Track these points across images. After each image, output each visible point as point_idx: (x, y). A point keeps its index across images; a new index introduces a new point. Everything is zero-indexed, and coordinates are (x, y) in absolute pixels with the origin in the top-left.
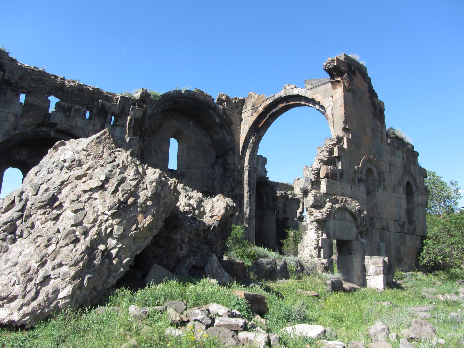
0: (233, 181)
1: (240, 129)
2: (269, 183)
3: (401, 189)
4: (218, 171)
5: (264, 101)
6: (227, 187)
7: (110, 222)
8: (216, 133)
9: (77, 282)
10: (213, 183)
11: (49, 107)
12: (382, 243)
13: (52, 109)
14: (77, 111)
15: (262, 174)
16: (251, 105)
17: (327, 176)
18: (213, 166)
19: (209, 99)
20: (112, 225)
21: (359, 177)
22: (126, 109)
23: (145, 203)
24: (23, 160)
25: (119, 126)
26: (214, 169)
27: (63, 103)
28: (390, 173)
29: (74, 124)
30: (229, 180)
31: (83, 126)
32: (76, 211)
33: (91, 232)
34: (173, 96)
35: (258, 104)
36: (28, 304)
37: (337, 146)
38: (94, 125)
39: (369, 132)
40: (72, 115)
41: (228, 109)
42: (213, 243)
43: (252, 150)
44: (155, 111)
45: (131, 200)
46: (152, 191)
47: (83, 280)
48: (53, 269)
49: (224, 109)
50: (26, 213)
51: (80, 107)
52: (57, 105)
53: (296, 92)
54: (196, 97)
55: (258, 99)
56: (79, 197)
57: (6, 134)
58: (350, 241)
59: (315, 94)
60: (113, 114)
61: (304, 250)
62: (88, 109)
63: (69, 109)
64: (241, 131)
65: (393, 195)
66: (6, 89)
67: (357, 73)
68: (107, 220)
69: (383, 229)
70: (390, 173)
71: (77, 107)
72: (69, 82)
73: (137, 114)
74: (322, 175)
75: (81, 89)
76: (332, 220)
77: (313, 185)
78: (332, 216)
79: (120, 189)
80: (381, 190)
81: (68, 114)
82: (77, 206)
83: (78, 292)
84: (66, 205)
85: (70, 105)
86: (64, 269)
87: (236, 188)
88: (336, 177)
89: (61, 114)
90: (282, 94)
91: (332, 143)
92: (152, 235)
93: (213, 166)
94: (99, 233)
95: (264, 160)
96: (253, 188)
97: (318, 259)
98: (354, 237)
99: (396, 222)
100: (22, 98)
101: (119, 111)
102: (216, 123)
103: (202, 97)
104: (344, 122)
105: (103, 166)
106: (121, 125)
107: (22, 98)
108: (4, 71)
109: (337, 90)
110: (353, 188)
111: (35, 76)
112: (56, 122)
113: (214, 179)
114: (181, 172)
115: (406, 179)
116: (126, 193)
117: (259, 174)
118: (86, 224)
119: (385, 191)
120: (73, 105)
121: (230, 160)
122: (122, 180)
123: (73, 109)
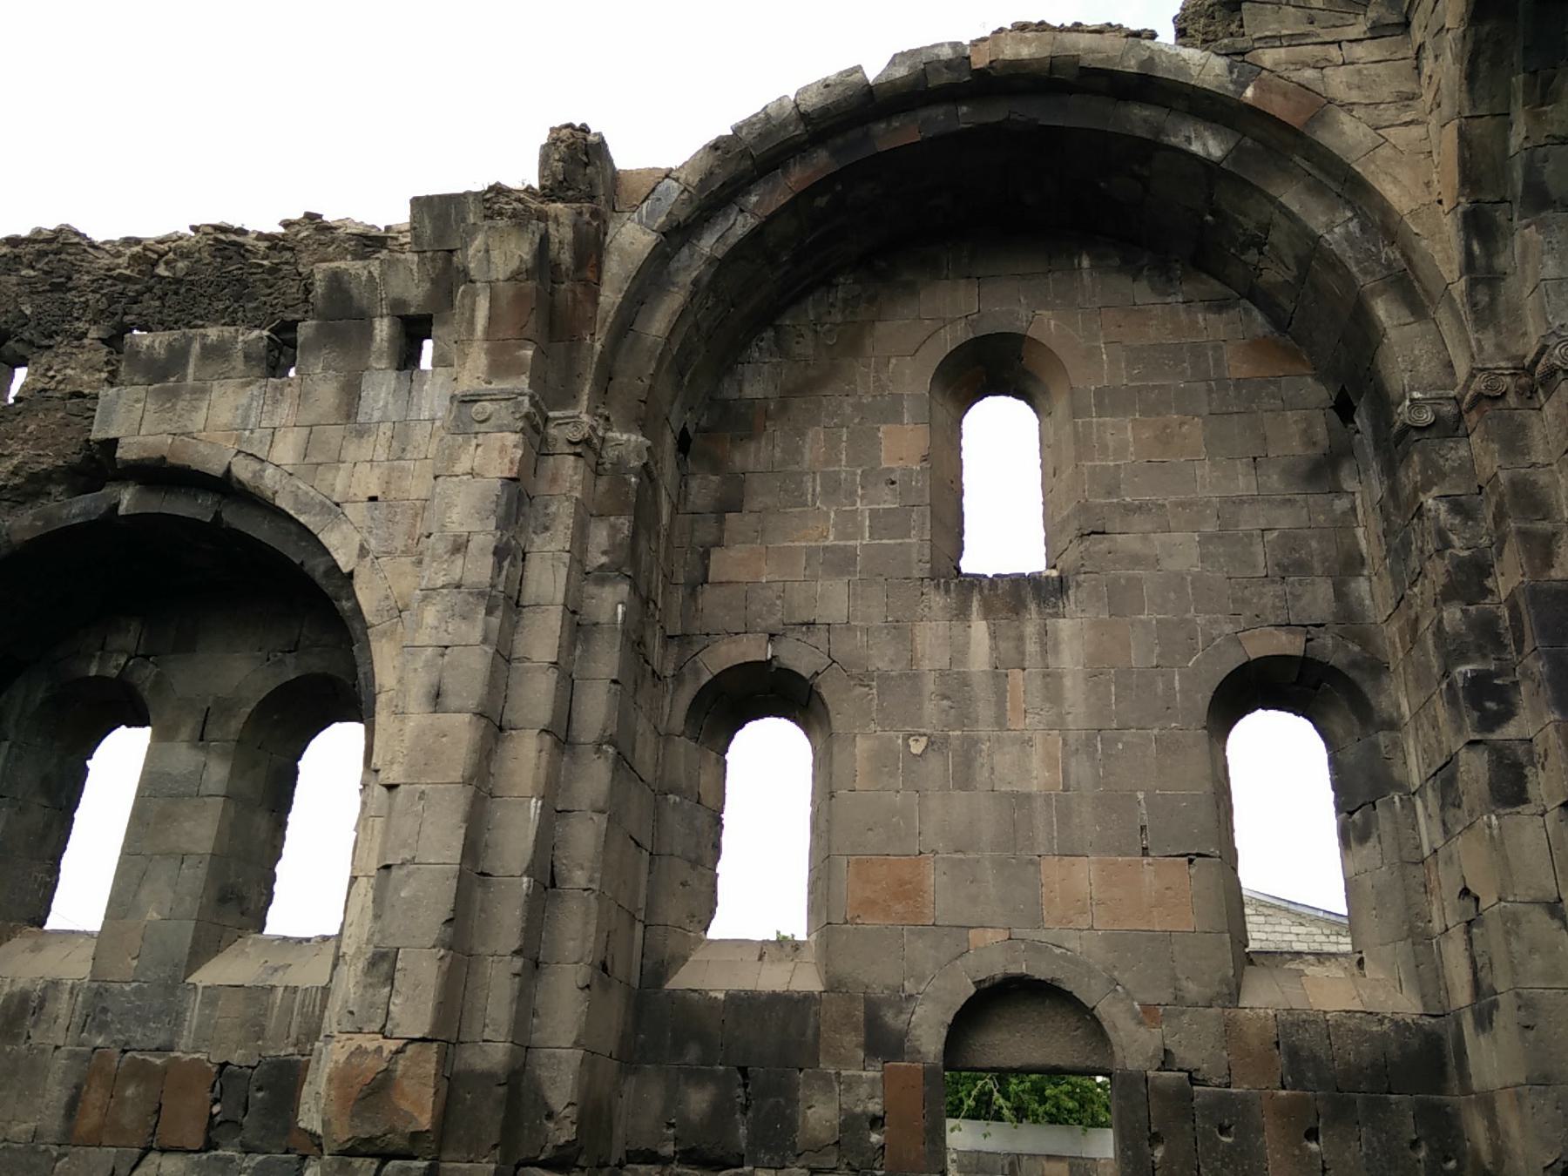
0: (1457, 506)
8: (1259, 244)
10: (1340, 594)
18: (1321, 472)
24: (114, 673)
26: (1338, 491)
30: (1420, 512)
38: (302, 397)
40: (190, 380)
54: (980, 61)
71: (213, 333)
73: (496, 255)
89: (140, 391)
102: (1205, 163)
103: (1025, 52)
111: (33, 268)
112: (112, 434)
113: (1352, 563)
123: (196, 347)
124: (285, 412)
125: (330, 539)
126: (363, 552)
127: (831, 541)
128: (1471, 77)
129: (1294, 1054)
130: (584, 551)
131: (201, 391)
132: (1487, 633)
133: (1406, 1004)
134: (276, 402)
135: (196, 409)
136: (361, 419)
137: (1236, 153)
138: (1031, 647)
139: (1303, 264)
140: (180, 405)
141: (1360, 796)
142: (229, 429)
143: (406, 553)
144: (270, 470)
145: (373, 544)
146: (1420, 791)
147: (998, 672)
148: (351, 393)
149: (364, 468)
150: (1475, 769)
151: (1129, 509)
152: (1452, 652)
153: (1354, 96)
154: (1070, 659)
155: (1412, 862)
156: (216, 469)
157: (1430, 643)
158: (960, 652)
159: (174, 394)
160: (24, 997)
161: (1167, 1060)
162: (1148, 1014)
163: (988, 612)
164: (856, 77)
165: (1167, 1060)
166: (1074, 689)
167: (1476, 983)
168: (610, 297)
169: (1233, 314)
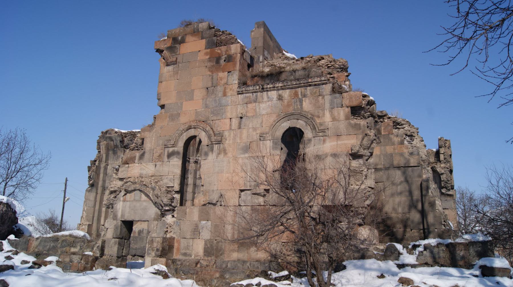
3: (269, 144)
12: (204, 222)
28: (240, 128)
39: (199, 94)
65: (242, 156)
67: (189, 38)
69: (214, 205)
70: (240, 128)
76: (121, 203)
80: (211, 157)
88: (135, 159)
98: (153, 216)
99: (249, 192)
108: (112, 140)
110: (157, 166)
115: (286, 125)
119: (222, 156)
130: (196, 175)
160: (140, 230)
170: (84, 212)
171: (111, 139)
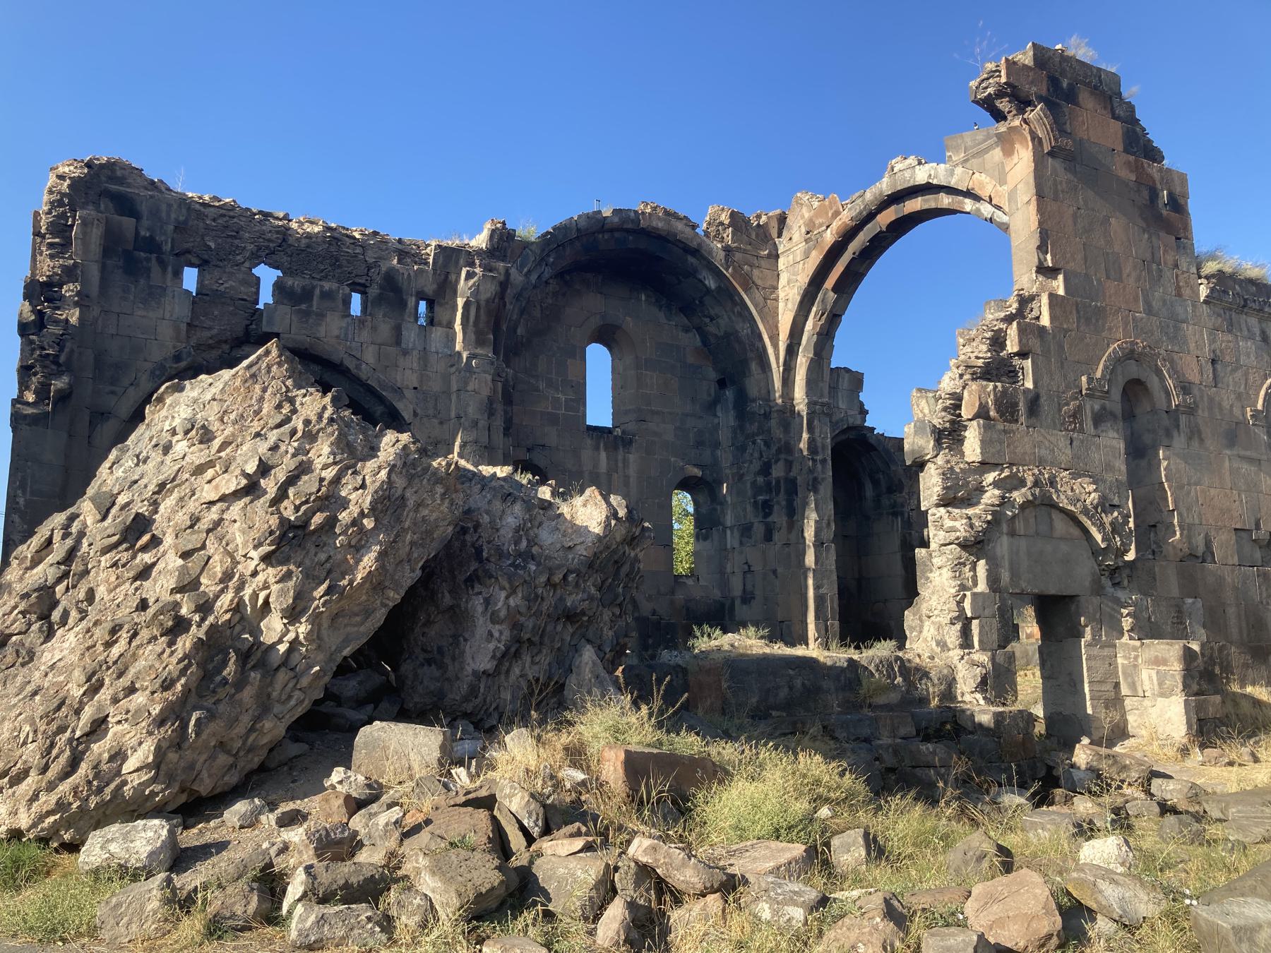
0: (767, 444)
1: (776, 300)
2: (872, 441)
4: (726, 419)
5: (837, 214)
6: (751, 462)
7: (261, 578)
9: (168, 730)
11: (257, 293)
13: (266, 297)
14: (327, 295)
15: (851, 420)
16: (803, 230)
17: (982, 413)
19: (680, 226)
20: (266, 586)
21: (1097, 407)
22: (453, 277)
23: (354, 522)
25: (440, 324)
26: (715, 415)
27: (290, 282)
29: (322, 332)
30: (754, 443)
31: (346, 334)
32: (185, 555)
33: (218, 604)
34: (578, 230)
35: (821, 225)
36: (51, 787)
37: (1015, 323)
41: (738, 249)
42: (585, 618)
43: (815, 354)
44: (534, 278)
45: (318, 519)
46: (376, 492)
47: (184, 726)
48: (115, 701)
49: (727, 249)
50: (76, 567)
51: (335, 286)
52: (279, 287)
53: (921, 175)
54: (643, 224)
55: (820, 212)
56: (195, 520)
57: (157, 373)
58: (1072, 598)
59: (977, 175)
60: (421, 296)
61: (922, 627)
62: (356, 287)
63: (306, 295)
64: (781, 305)
66: (148, 260)
68: (255, 574)
71: (327, 286)
72: (301, 224)
74: (966, 413)
75: (335, 239)
77: (938, 442)
78: (1005, 528)
79: (291, 491)
81: (303, 307)
82: (192, 541)
83: (172, 756)
84: (168, 540)
85: (307, 282)
86: (140, 699)
87: (776, 462)
89: (285, 309)
90: (885, 186)
91: (1002, 315)
92: (386, 605)
93: (711, 407)
94: (237, 608)
95: (857, 380)
96: (824, 461)
97: (960, 652)
100: (190, 279)
101: (435, 286)
102: (708, 290)
103: (660, 225)
104: (1039, 248)
105: (258, 435)
106: (445, 323)
107: (190, 279)
109: (1015, 158)
111: (214, 220)
114: (623, 432)
116: (307, 502)
117: (842, 420)
118: (208, 585)
120: (315, 283)
121: (753, 390)
122: (303, 469)
123: (317, 292)
124: (365, 335)
125: (400, 406)
126: (415, 414)
127: (550, 410)
128: (801, 302)
129: (688, 609)
131: (321, 316)
132: (768, 487)
133: (717, 594)
134: (360, 329)
135: (320, 325)
136: (403, 346)
137: (719, 288)
138: (620, 465)
139: (727, 335)
140: (311, 321)
141: (705, 524)
142: (338, 337)
143: (435, 417)
144: (364, 366)
145: (419, 411)
146: (731, 528)
147: (609, 475)
148: (398, 330)
149: (408, 372)
150: (759, 529)
151: (653, 413)
152: (757, 490)
153: (759, 282)
154: (632, 471)
155: (723, 550)
156: (335, 358)
157: (749, 485)
158: (596, 465)
159: (307, 314)
161: (654, 613)
162: (649, 599)
163: (606, 449)
164: (598, 216)
165: (654, 613)
166: (633, 481)
167: (744, 590)
168: (509, 307)
169: (690, 335)
170: (16, 518)
171: (125, 205)
